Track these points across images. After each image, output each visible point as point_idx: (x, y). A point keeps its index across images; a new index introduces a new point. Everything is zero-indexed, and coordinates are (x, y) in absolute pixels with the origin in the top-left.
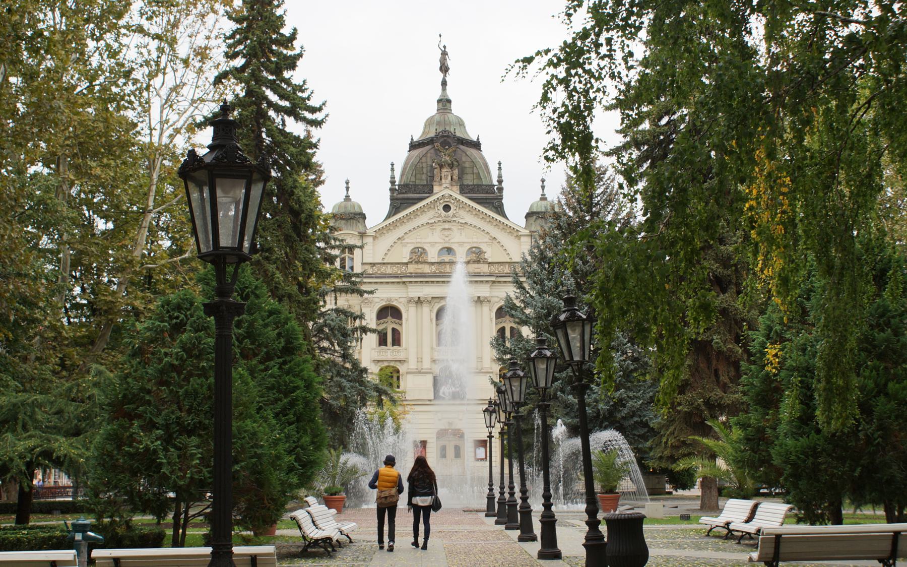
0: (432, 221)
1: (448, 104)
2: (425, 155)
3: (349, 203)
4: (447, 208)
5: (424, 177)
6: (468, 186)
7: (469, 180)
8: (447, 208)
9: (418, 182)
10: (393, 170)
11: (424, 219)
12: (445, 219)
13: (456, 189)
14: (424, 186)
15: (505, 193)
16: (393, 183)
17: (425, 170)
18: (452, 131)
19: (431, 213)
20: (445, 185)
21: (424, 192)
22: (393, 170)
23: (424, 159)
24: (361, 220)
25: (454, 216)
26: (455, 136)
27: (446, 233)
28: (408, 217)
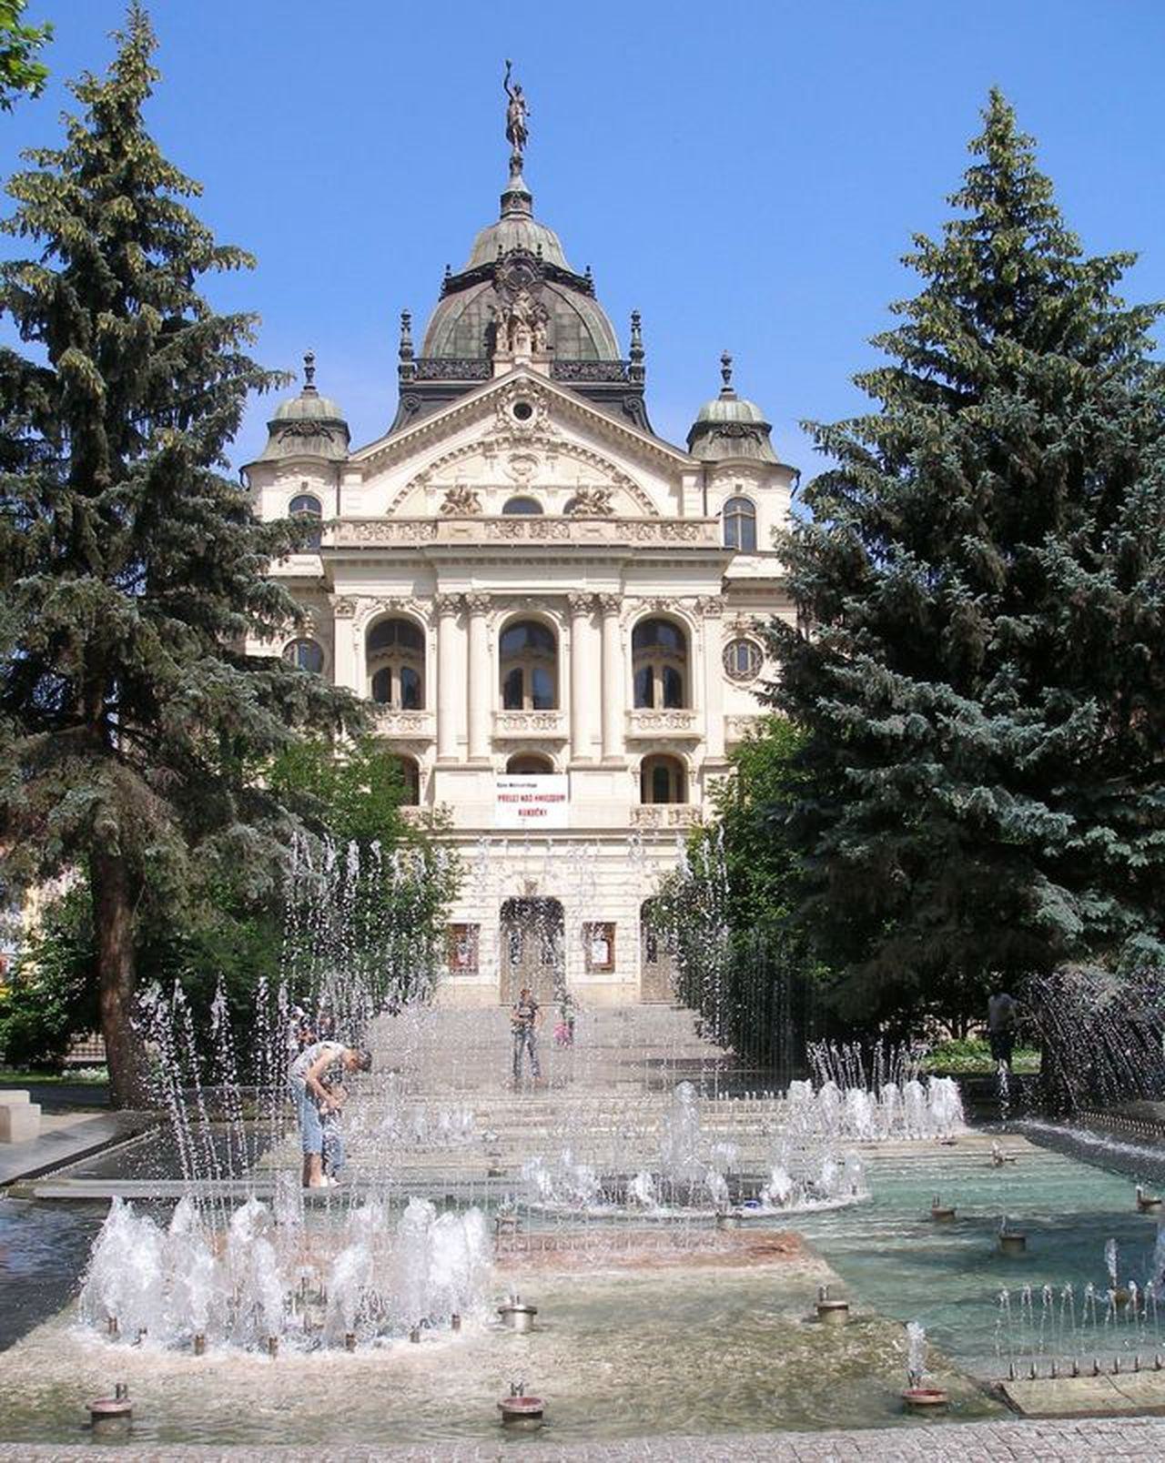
0: (491, 438)
1: (525, 205)
2: (475, 301)
3: (312, 403)
4: (523, 411)
5: (474, 344)
6: (568, 363)
7: (569, 352)
8: (523, 411)
9: (460, 355)
10: (406, 326)
11: (473, 434)
12: (517, 434)
13: (544, 369)
14: (473, 362)
15: (649, 381)
16: (405, 354)
17: (475, 331)
18: (535, 251)
19: (489, 422)
20: (518, 361)
21: (474, 377)
22: (406, 326)
23: (474, 309)
24: (337, 437)
25: (538, 428)
26: (539, 261)
27: (520, 465)
28: (439, 433)
